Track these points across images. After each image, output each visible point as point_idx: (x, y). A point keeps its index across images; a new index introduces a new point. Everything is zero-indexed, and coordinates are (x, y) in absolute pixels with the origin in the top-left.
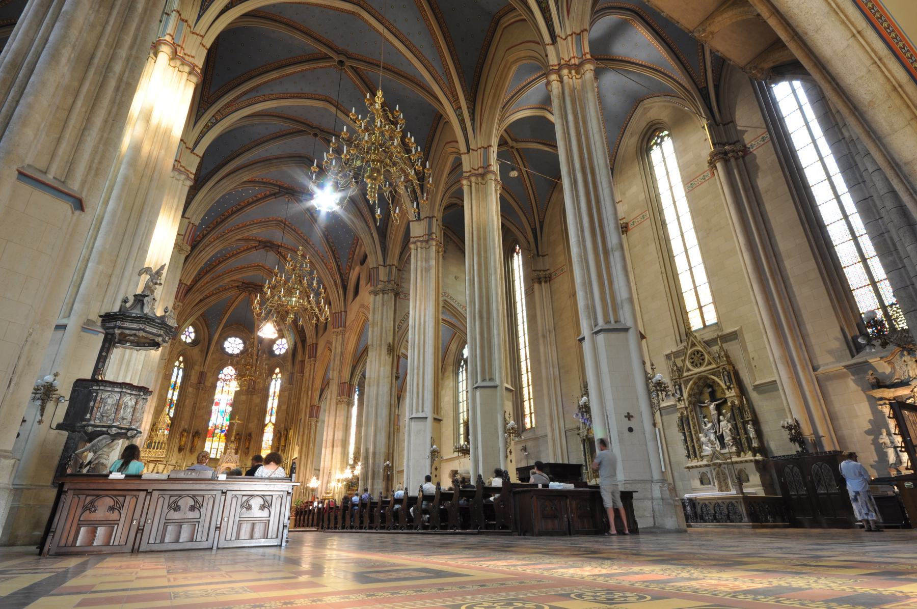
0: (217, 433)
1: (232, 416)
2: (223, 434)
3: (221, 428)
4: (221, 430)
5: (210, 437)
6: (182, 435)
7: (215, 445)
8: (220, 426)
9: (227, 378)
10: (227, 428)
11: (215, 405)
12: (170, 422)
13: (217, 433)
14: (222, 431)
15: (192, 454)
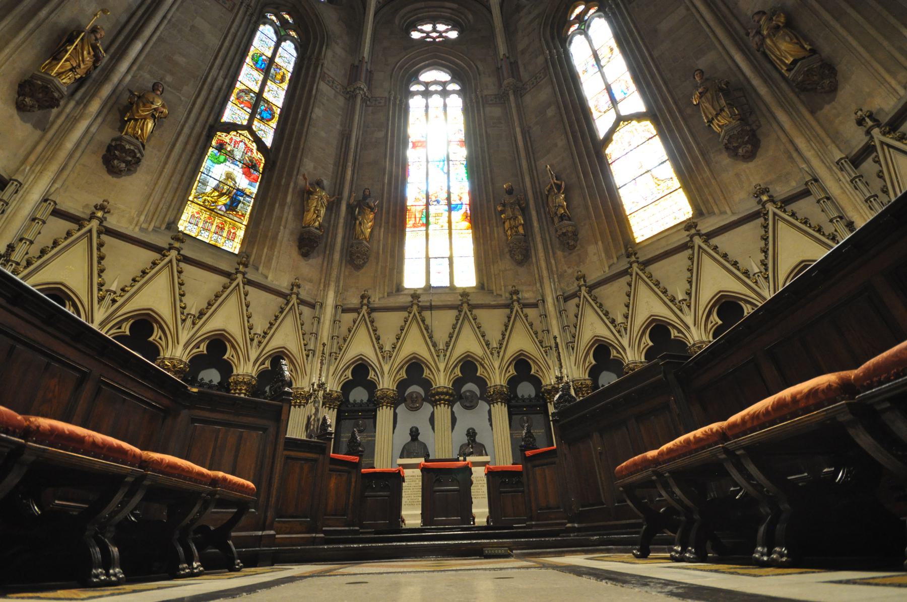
0: (438, 215)
1: (475, 167)
2: (458, 216)
3: (449, 199)
4: (449, 203)
5: (414, 226)
6: (305, 195)
7: (439, 244)
8: (443, 196)
9: (433, 88)
10: (466, 199)
11: (414, 146)
12: (258, 156)
13: (438, 215)
14: (451, 208)
15: (358, 268)
